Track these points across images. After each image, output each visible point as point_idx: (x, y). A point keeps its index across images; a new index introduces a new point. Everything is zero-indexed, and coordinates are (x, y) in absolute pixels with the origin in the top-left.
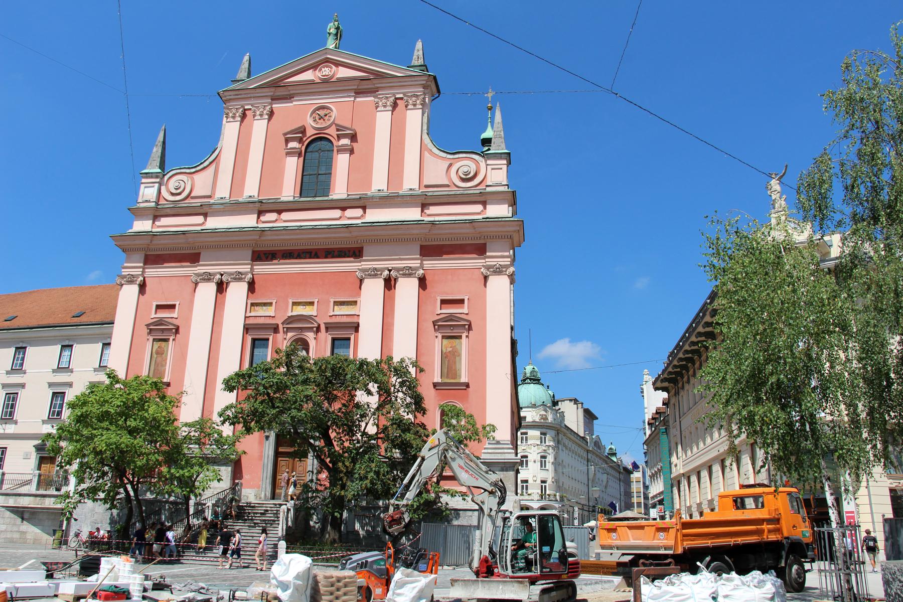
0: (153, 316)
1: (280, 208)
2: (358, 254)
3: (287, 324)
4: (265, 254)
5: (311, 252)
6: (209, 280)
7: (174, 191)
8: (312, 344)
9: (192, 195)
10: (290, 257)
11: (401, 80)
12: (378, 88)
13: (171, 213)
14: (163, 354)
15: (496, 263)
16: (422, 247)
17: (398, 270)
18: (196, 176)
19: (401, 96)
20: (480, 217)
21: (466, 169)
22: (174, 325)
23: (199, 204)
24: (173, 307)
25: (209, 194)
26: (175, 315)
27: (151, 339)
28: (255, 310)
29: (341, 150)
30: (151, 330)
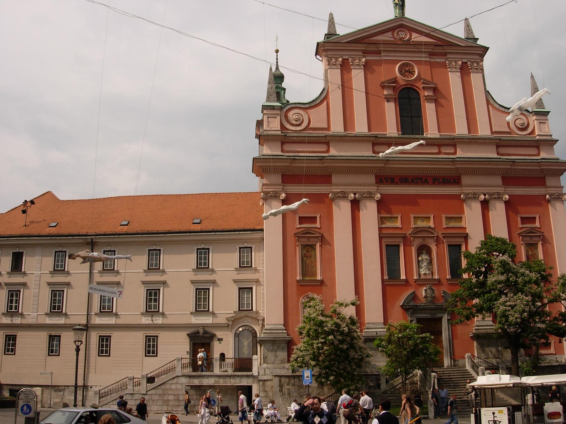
1: (389, 142)
2: (457, 181)
4: (385, 178)
5: (422, 179)
7: (294, 123)
8: (434, 248)
9: (310, 126)
10: (405, 183)
11: (463, 49)
12: (446, 52)
13: (296, 141)
14: (312, 257)
15: (556, 192)
16: (503, 178)
17: (490, 195)
18: (310, 111)
19: (465, 61)
20: (539, 158)
21: (521, 122)
22: (319, 233)
23: (324, 135)
24: (313, 220)
25: (326, 126)
26: (318, 225)
29: (428, 99)
30: (299, 237)
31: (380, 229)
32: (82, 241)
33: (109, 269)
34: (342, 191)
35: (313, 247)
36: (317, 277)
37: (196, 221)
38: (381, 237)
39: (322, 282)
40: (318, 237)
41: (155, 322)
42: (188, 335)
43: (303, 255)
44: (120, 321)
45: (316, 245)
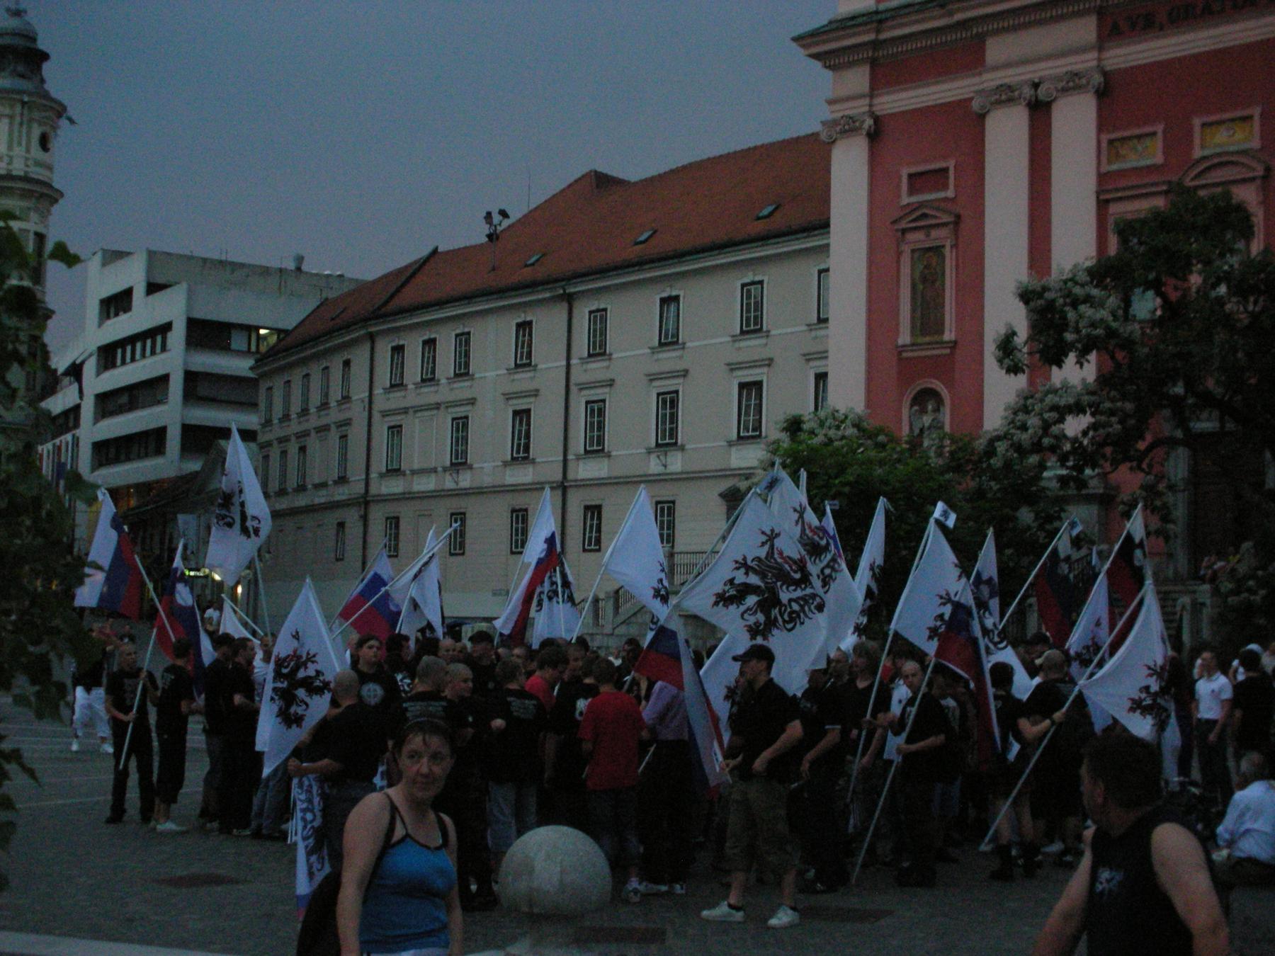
0: (905, 200)
3: (1192, 179)
6: (1010, 100)
26: (950, 193)
27: (907, 249)
28: (1118, 155)
30: (904, 231)
31: (1102, 178)
32: (547, 295)
33: (598, 351)
34: (1001, 86)
35: (937, 250)
36: (941, 332)
37: (761, 215)
38: (1107, 201)
39: (954, 345)
40: (945, 224)
41: (671, 469)
42: (722, 495)
43: (917, 274)
44: (620, 470)
45: (943, 246)
